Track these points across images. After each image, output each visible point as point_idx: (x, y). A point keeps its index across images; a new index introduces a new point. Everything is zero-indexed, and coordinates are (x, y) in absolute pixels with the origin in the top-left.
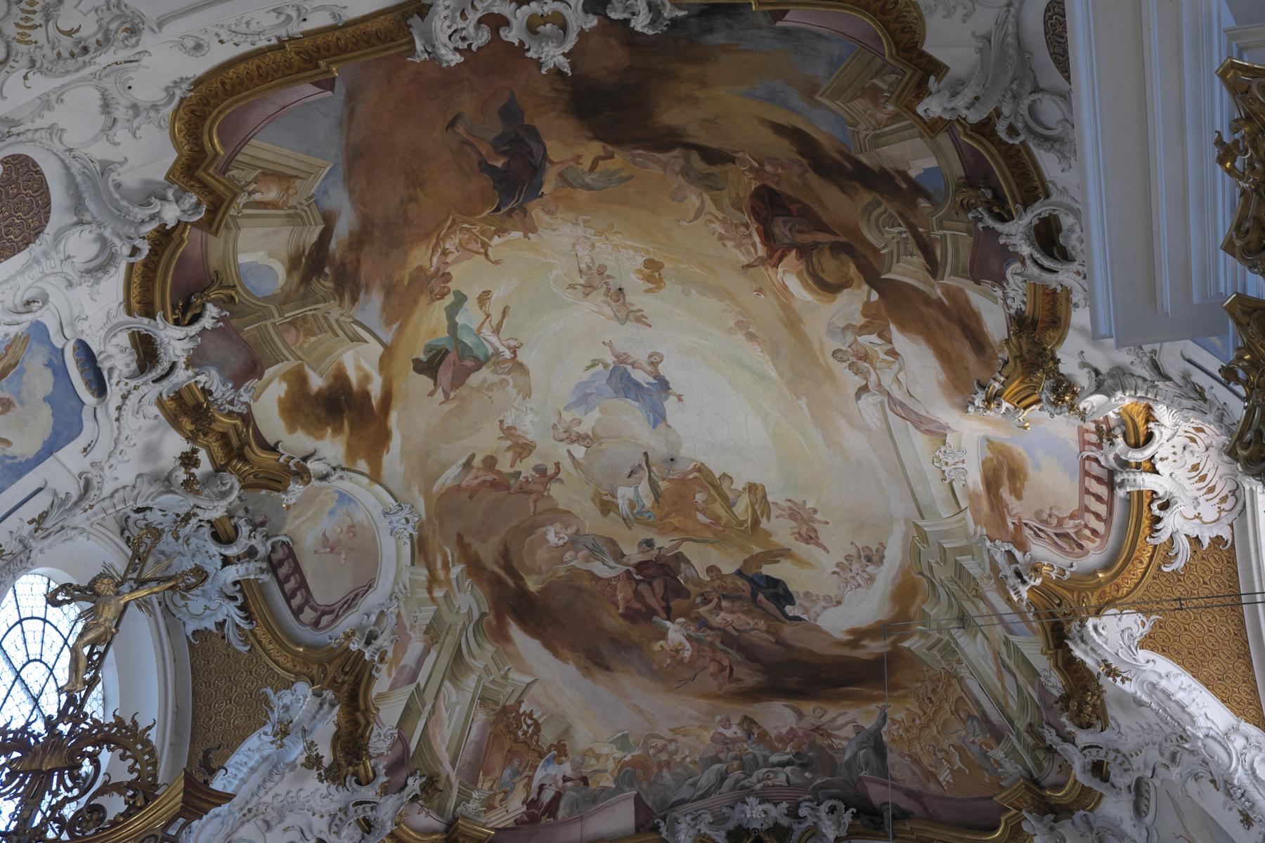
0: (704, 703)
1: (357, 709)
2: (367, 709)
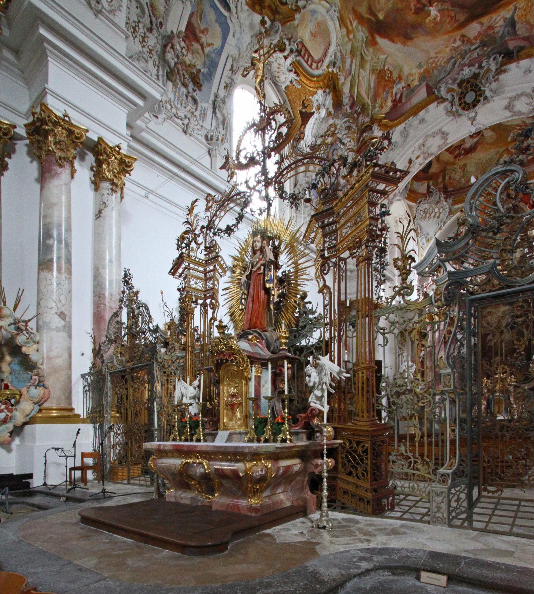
0: (445, 37)
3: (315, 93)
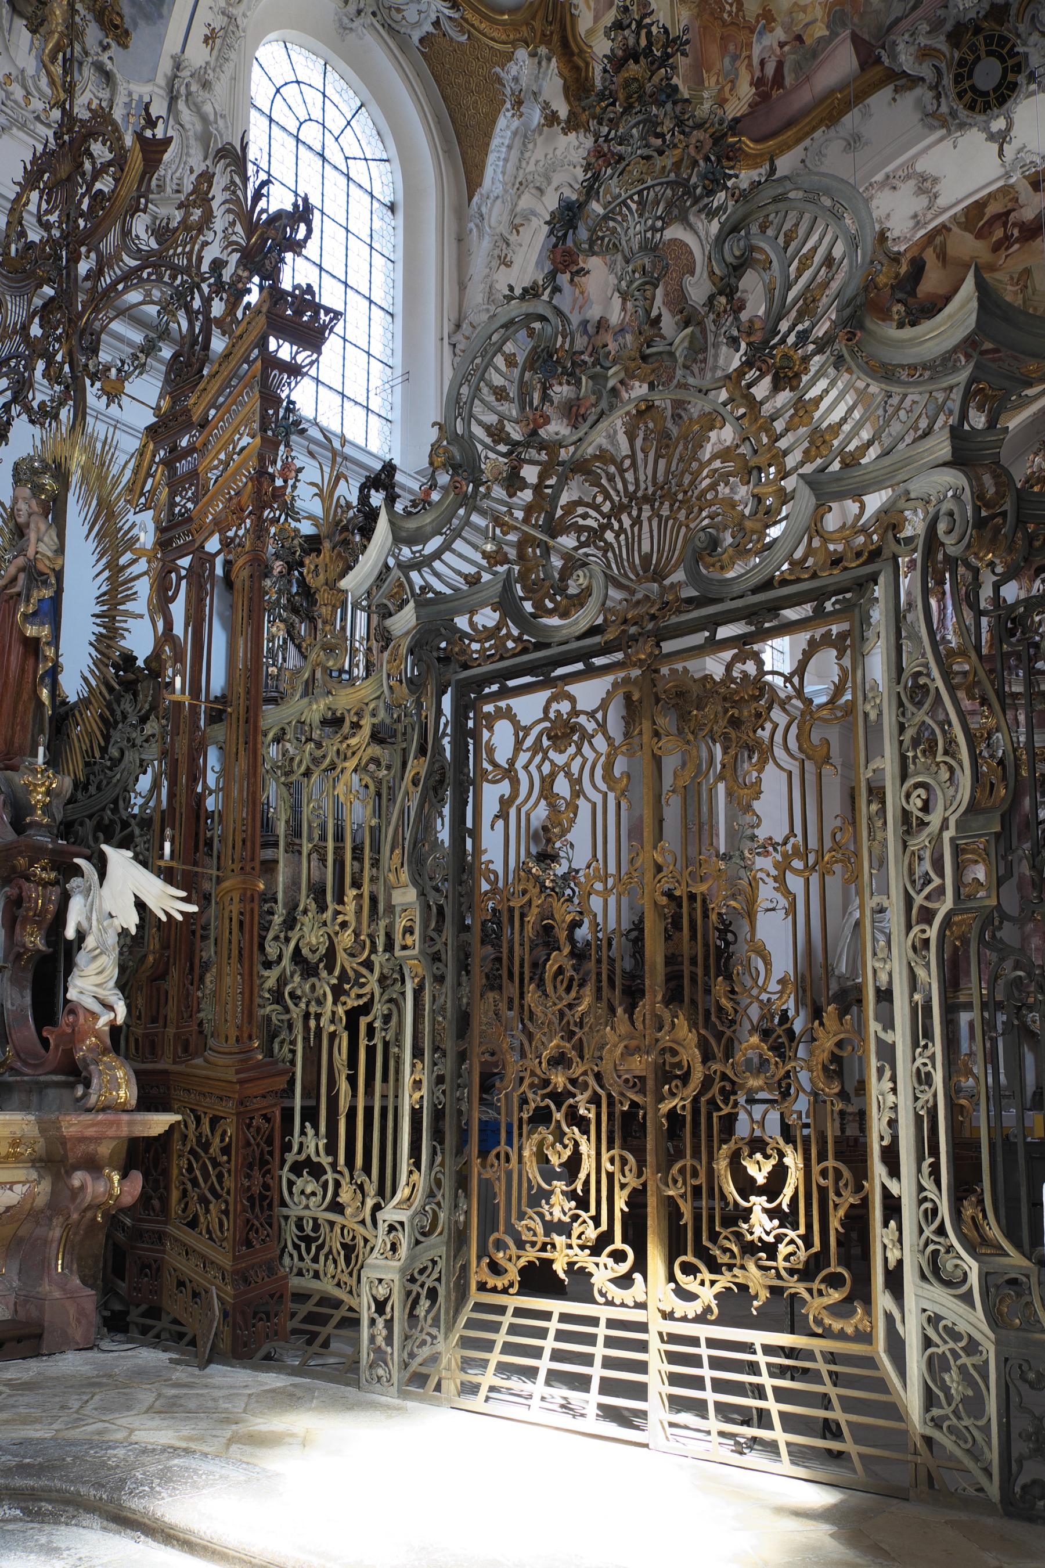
1: (572, 54)
2: (581, 51)
3: (510, 57)
